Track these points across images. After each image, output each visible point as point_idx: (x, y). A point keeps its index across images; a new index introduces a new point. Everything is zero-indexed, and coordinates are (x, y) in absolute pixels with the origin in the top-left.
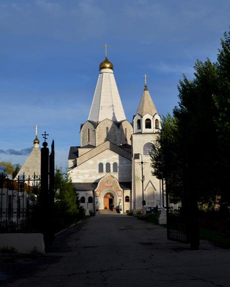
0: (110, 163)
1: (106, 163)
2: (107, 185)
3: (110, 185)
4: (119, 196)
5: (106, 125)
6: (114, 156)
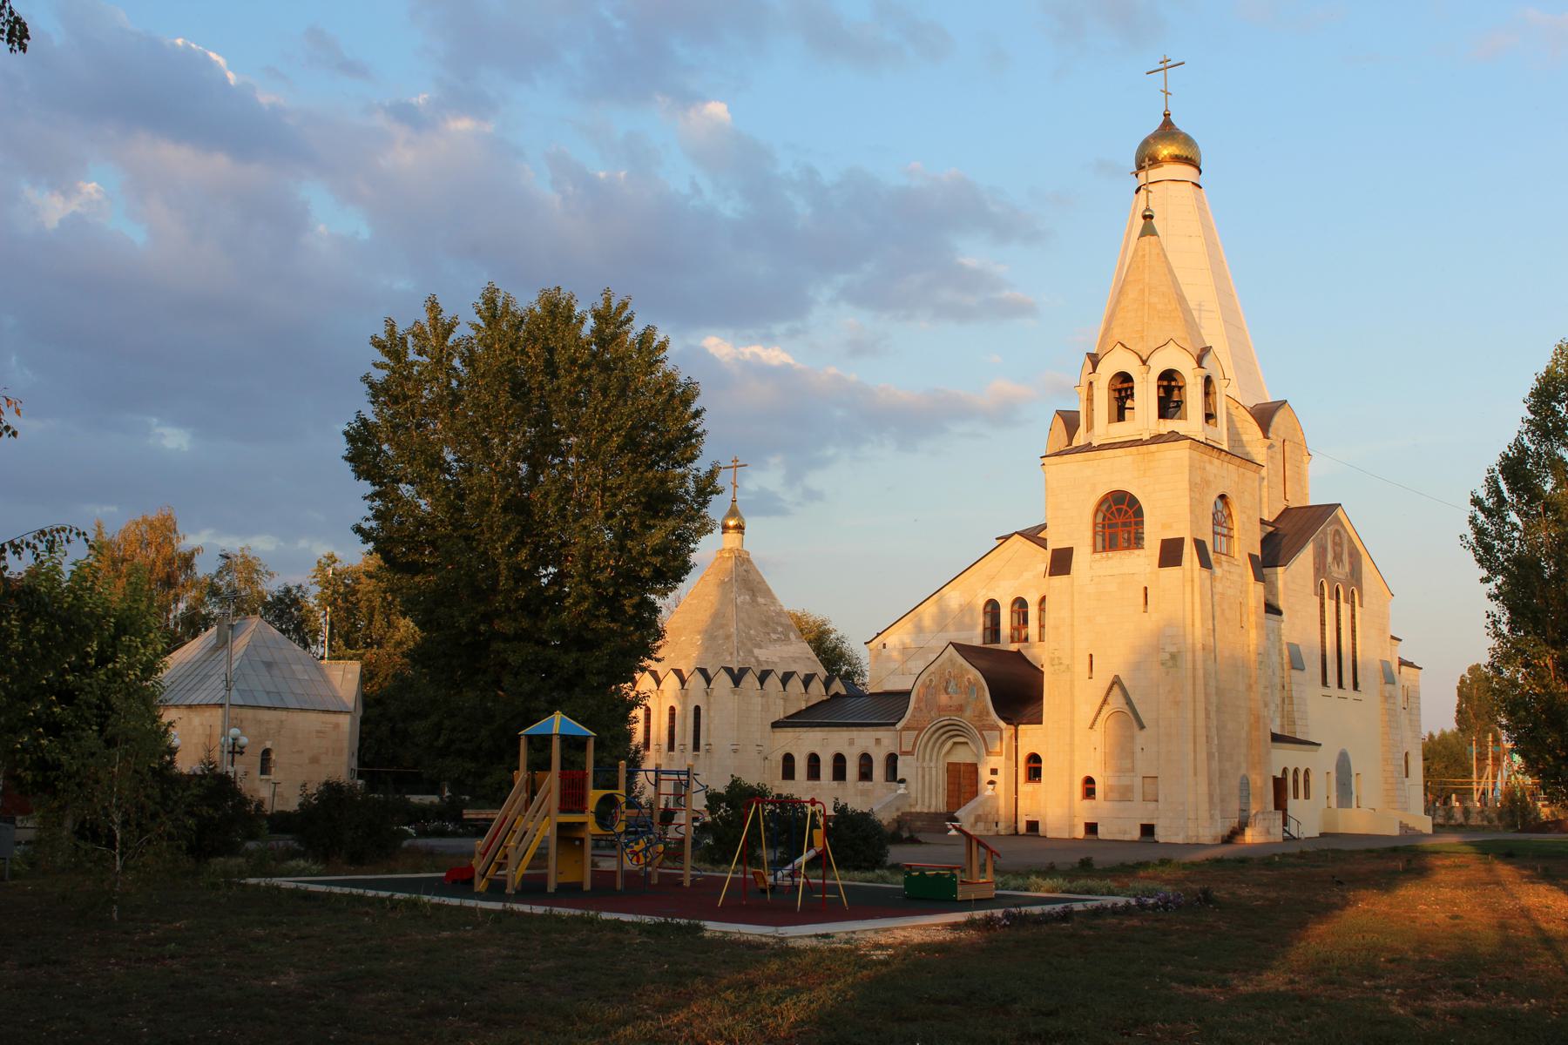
2: (943, 699)
3: (957, 699)
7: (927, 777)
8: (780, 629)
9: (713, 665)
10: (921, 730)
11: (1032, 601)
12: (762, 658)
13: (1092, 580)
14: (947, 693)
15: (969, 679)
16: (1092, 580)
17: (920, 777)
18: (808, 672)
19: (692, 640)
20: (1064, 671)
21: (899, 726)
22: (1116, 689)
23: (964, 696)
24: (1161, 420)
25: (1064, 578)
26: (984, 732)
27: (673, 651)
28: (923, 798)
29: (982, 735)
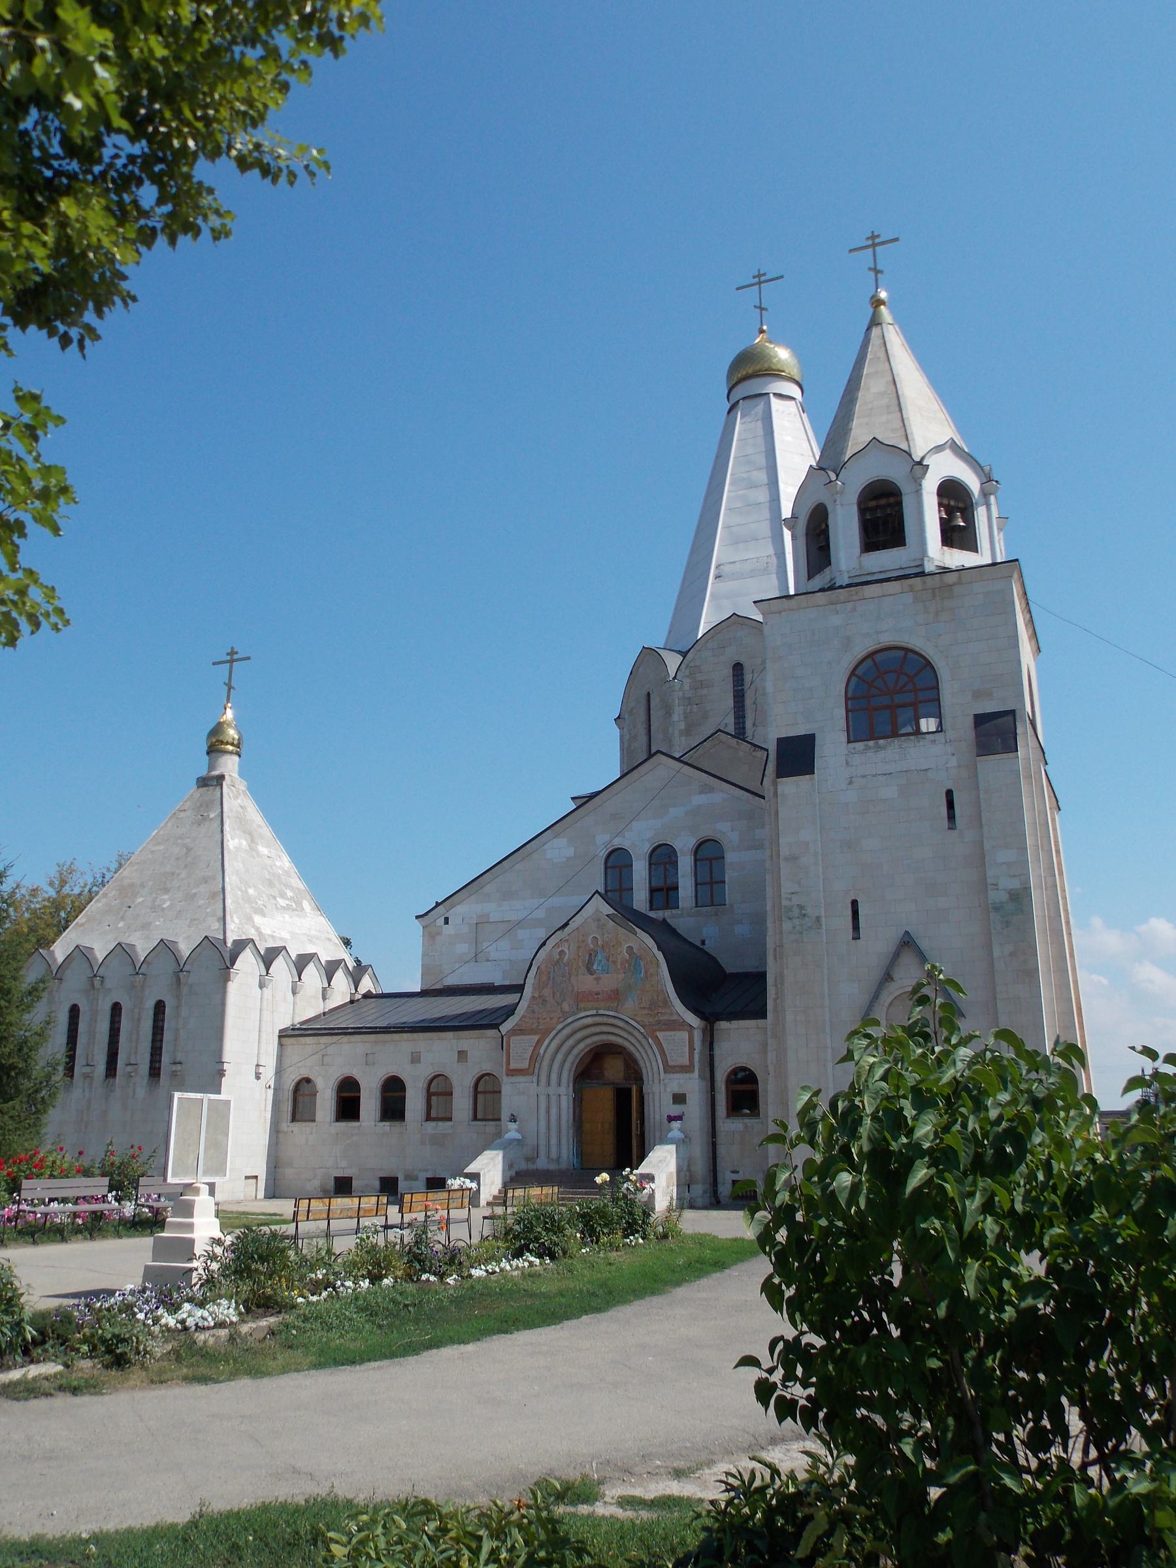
0: (677, 845)
1: (647, 848)
2: (586, 983)
3: (610, 981)
4: (669, 1069)
5: (732, 654)
6: (700, 800)
7: (554, 1111)
8: (289, 894)
9: (188, 937)
10: (545, 1033)
11: (684, 845)
12: (266, 931)
13: (851, 783)
14: (591, 972)
15: (630, 948)
16: (851, 783)
17: (543, 1110)
18: (329, 959)
19: (154, 901)
20: (810, 928)
21: (505, 1028)
22: (908, 959)
23: (622, 976)
24: (945, 548)
25: (803, 780)
26: (660, 1035)
27: (122, 918)
28: (549, 1145)
29: (656, 1039)
